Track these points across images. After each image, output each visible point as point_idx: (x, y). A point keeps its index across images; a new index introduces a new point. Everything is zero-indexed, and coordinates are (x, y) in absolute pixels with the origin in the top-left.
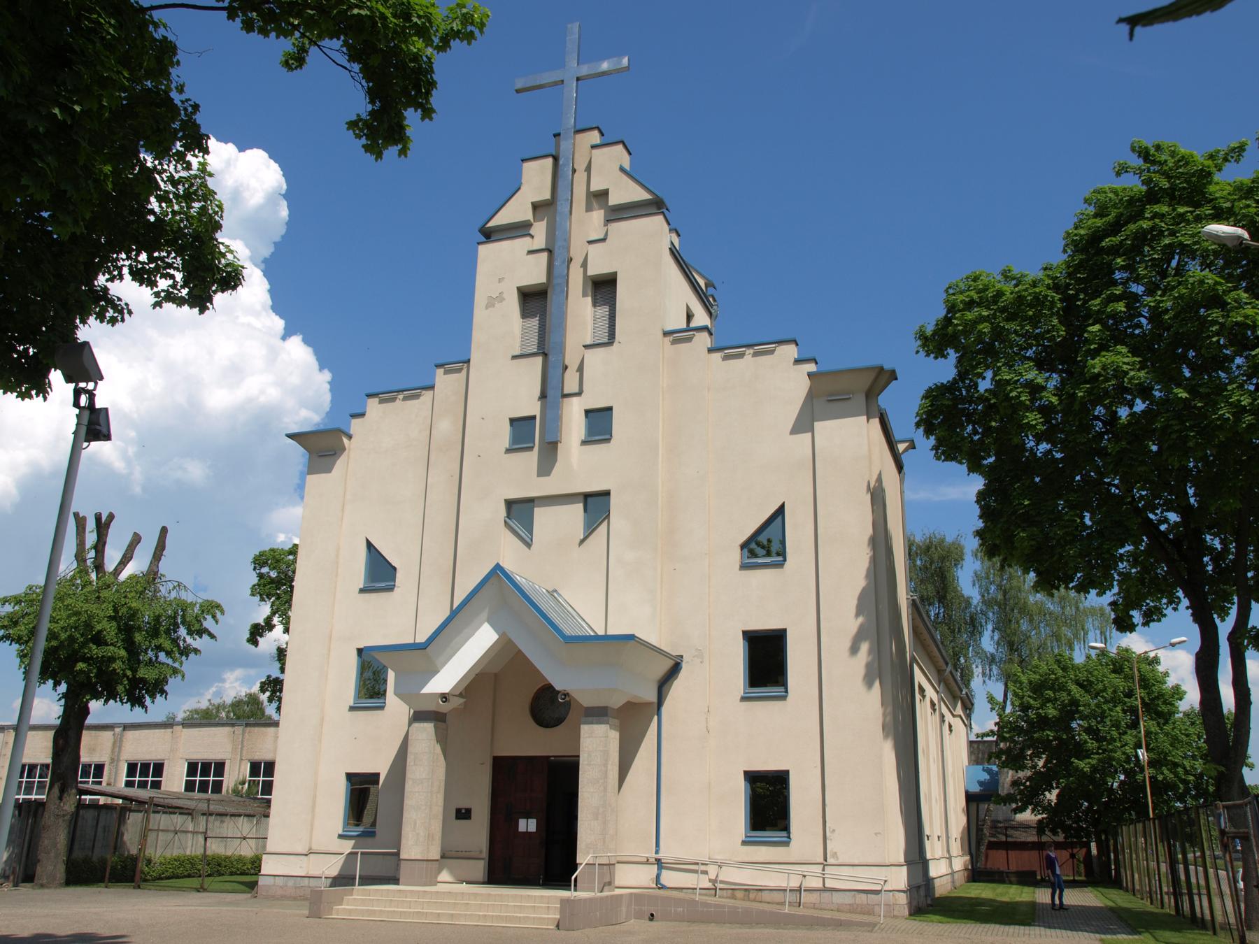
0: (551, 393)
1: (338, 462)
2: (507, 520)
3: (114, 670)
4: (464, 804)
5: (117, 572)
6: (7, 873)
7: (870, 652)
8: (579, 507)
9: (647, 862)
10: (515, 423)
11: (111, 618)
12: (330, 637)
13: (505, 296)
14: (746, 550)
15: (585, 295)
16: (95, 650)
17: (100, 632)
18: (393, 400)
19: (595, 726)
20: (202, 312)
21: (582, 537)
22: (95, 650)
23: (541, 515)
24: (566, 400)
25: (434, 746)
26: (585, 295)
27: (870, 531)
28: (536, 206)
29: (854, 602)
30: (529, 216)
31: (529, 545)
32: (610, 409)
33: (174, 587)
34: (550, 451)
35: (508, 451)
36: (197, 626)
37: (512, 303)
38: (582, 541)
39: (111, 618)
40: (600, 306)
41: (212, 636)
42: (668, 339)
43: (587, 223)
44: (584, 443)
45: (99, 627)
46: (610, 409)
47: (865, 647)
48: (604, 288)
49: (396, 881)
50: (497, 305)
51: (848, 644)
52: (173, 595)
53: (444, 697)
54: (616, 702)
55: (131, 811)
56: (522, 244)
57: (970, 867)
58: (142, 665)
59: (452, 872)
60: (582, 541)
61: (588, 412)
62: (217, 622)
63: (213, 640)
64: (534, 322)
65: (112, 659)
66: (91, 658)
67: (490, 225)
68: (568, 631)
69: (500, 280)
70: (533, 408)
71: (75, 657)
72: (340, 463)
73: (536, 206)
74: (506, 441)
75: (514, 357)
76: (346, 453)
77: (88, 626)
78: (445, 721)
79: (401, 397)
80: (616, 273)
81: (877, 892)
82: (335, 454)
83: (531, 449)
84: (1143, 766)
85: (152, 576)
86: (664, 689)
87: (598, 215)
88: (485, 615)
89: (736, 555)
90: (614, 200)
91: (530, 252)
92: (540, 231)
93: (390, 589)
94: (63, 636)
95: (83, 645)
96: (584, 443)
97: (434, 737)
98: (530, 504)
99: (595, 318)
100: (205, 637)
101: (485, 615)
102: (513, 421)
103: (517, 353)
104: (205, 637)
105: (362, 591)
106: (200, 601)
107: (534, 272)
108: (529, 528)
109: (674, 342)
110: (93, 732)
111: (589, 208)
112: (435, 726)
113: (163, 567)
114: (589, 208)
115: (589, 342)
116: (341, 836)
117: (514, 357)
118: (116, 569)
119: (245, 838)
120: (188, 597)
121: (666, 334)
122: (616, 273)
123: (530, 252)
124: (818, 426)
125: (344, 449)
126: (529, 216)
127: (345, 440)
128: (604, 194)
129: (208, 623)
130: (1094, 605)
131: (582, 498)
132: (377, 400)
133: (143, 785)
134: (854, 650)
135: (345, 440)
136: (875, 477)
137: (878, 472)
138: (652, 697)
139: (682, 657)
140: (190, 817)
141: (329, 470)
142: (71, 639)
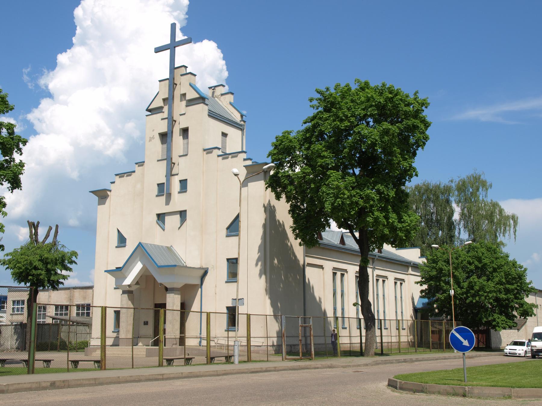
0: (170, 174)
1: (107, 200)
2: (158, 221)
3: (41, 278)
4: (146, 320)
5: (44, 242)
6: (19, 347)
7: (261, 265)
8: (178, 216)
9: (197, 338)
10: (159, 185)
11: (39, 260)
12: (107, 264)
13: (155, 137)
14: (228, 230)
15: (180, 135)
16: (34, 272)
17: (35, 266)
18: (123, 177)
19: (171, 294)
20: (6, 204)
21: (179, 226)
22: (34, 272)
23: (167, 218)
24: (173, 177)
25: (128, 302)
26: (180, 135)
27: (263, 222)
28: (164, 100)
29: (257, 249)
30: (161, 104)
31: (164, 230)
32: (186, 180)
33: (62, 247)
34: (169, 196)
35: (157, 196)
36: (70, 261)
37: (157, 139)
38: (179, 228)
39: (39, 260)
40: (186, 139)
41: (76, 263)
42: (205, 152)
43: (179, 106)
44: (179, 193)
45: (35, 264)
46: (186, 180)
47: (260, 264)
48: (185, 132)
49: (119, 346)
50: (152, 140)
51: (255, 262)
52: (62, 249)
53: (129, 286)
54: (179, 286)
55: (62, 325)
56: (159, 116)
57: (413, 341)
58: (52, 275)
59: (142, 343)
60: (179, 228)
61: (181, 181)
62: (77, 258)
63: (76, 265)
64: (165, 146)
65: (41, 275)
66: (34, 274)
67: (149, 108)
68: (159, 265)
69: (153, 130)
70: (163, 180)
71: (28, 275)
72: (108, 201)
73: (164, 100)
74: (156, 192)
75: (158, 161)
76: (109, 197)
77: (31, 263)
78: (132, 293)
79: (126, 175)
80: (188, 127)
81: (260, 346)
82: (106, 197)
83: (163, 195)
84: (451, 297)
85: (54, 243)
86: (203, 279)
87: (184, 103)
88: (138, 259)
89: (224, 232)
90: (188, 97)
91: (162, 119)
92: (166, 109)
93: (125, 246)
94: (23, 268)
95: (30, 270)
96: (179, 193)
97: (128, 299)
98: (164, 215)
99: (184, 144)
100: (74, 264)
101: (138, 259)
102: (158, 185)
103: (160, 159)
104: (74, 264)
105: (116, 247)
106: (70, 251)
107: (164, 128)
108: (164, 223)
109: (207, 153)
110: (84, 290)
111: (181, 101)
112: (128, 296)
113: (59, 238)
114: (181, 101)
115: (181, 154)
116: (113, 332)
117: (158, 161)
118: (43, 241)
119: (88, 334)
120: (66, 250)
121: (204, 150)
122: (188, 127)
123: (162, 119)
124: (249, 184)
125: (108, 196)
126: (161, 104)
127: (109, 193)
128: (184, 95)
129: (74, 259)
130: (508, 214)
131: (179, 213)
132: (118, 177)
133: (61, 314)
134: (257, 265)
135: (109, 193)
136: (267, 202)
137: (268, 200)
138: (198, 282)
139: (208, 268)
140: (87, 327)
141: (104, 204)
142: (27, 269)
